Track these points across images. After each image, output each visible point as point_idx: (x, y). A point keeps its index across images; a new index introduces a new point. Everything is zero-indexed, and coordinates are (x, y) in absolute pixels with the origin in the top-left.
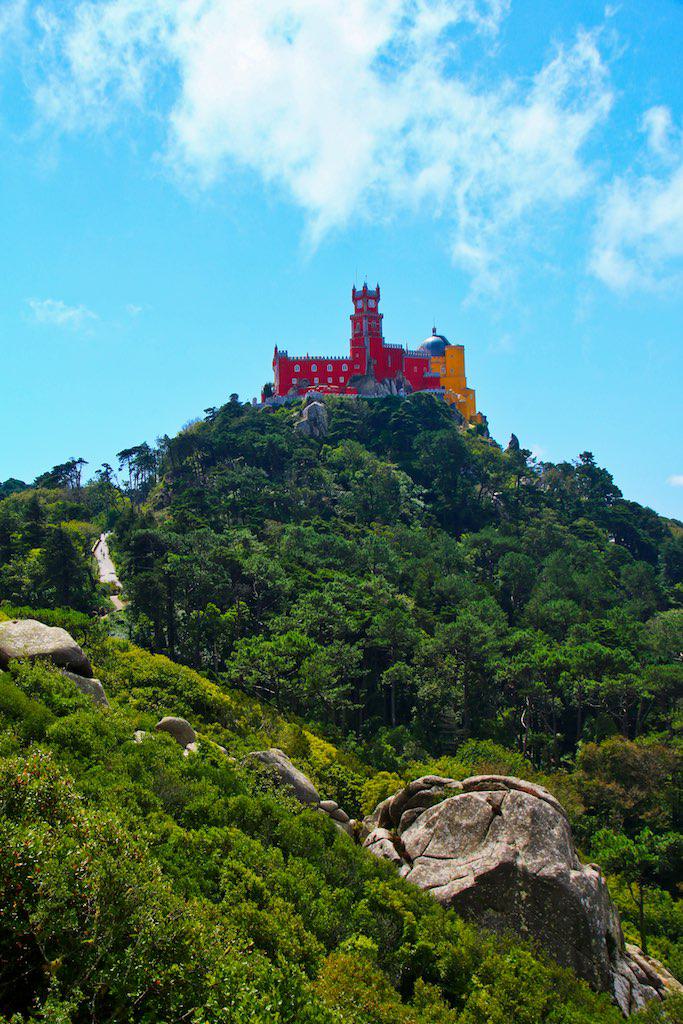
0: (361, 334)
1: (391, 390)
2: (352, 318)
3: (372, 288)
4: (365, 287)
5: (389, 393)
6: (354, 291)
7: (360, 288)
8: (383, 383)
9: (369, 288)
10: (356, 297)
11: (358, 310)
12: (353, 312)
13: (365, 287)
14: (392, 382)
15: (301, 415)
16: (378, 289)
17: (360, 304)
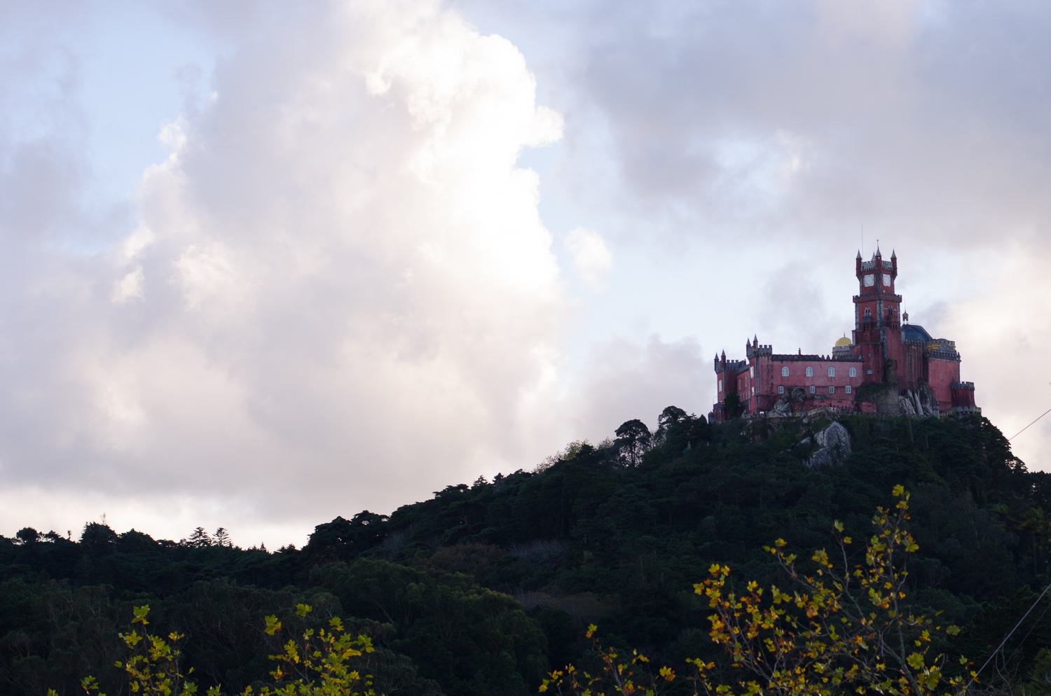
0: (873, 324)
1: (915, 405)
2: (856, 299)
3: (886, 258)
4: (878, 257)
5: (914, 412)
6: (859, 260)
7: (867, 258)
8: (904, 393)
9: (883, 259)
10: (861, 271)
11: (862, 287)
12: (857, 292)
13: (878, 257)
14: (916, 395)
15: (814, 441)
16: (894, 259)
17: (870, 280)
